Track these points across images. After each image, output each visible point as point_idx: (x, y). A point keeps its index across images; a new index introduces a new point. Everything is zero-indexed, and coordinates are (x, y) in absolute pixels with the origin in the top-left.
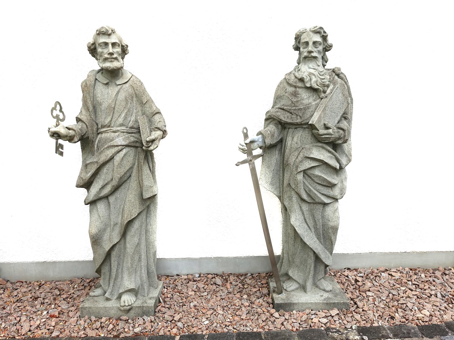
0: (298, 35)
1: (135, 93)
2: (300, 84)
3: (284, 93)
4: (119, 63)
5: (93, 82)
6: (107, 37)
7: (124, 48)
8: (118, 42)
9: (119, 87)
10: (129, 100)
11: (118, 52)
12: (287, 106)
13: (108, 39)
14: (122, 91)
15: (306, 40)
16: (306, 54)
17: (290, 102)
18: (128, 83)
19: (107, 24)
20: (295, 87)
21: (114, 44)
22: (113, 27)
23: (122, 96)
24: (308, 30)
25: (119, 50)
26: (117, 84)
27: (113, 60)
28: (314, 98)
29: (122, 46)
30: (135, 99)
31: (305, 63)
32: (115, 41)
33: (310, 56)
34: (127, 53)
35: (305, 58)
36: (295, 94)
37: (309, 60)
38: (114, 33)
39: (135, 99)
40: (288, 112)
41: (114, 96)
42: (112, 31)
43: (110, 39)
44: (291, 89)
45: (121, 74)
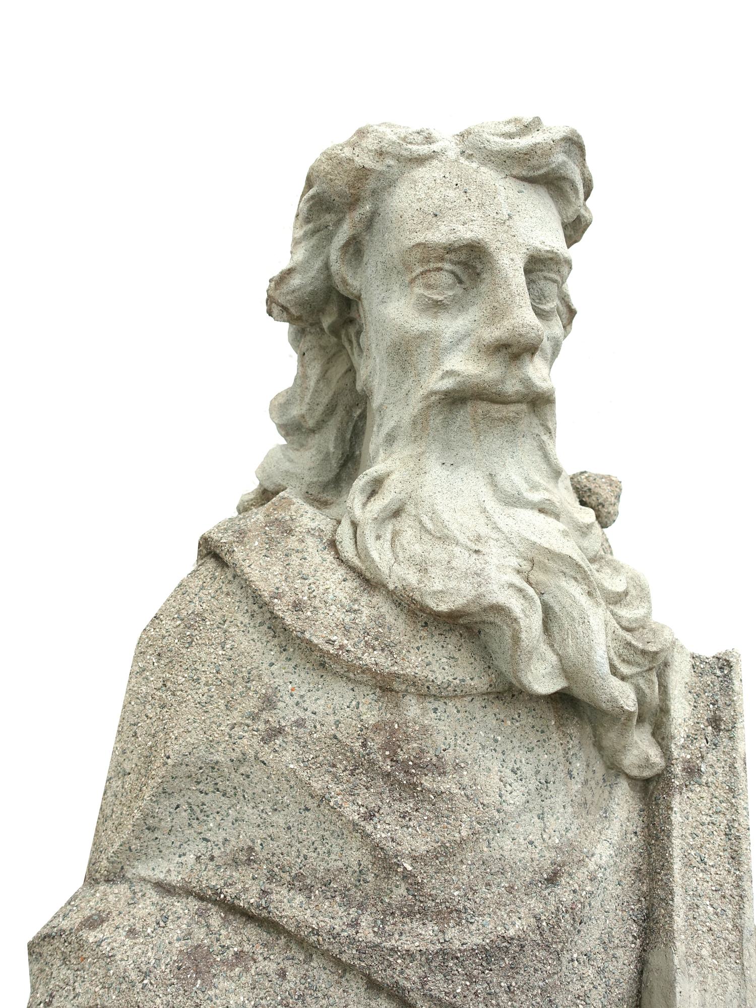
0: (363, 173)
2: (434, 661)
3: (249, 743)
12: (300, 883)
15: (466, 234)
16: (464, 366)
17: (355, 855)
20: (386, 686)
24: (446, 140)
28: (576, 786)
31: (447, 446)
33: (512, 387)
35: (457, 399)
36: (403, 772)
37: (493, 422)
40: (344, 968)
44: (335, 709)
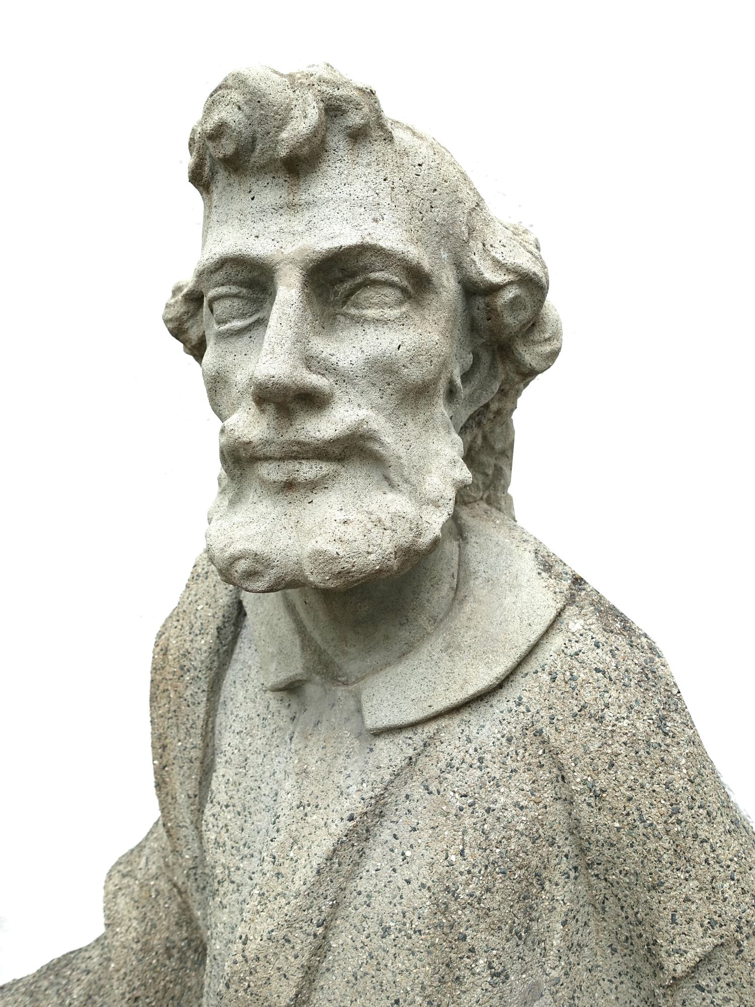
1: (574, 828)
4: (394, 503)
5: (205, 642)
6: (270, 194)
7: (491, 312)
8: (391, 237)
9: (391, 753)
10: (479, 938)
11: (383, 370)
13: (276, 223)
14: (416, 807)
18: (501, 705)
19: (289, 47)
21: (337, 279)
22: (356, 72)
23: (402, 876)
25: (416, 337)
26: (377, 718)
27: (308, 470)
29: (474, 291)
30: (561, 893)
32: (348, 238)
34: (529, 356)
38: (357, 136)
39: (561, 893)
41: (303, 875)
42: (333, 110)
43: (297, 223)
45: (445, 589)
